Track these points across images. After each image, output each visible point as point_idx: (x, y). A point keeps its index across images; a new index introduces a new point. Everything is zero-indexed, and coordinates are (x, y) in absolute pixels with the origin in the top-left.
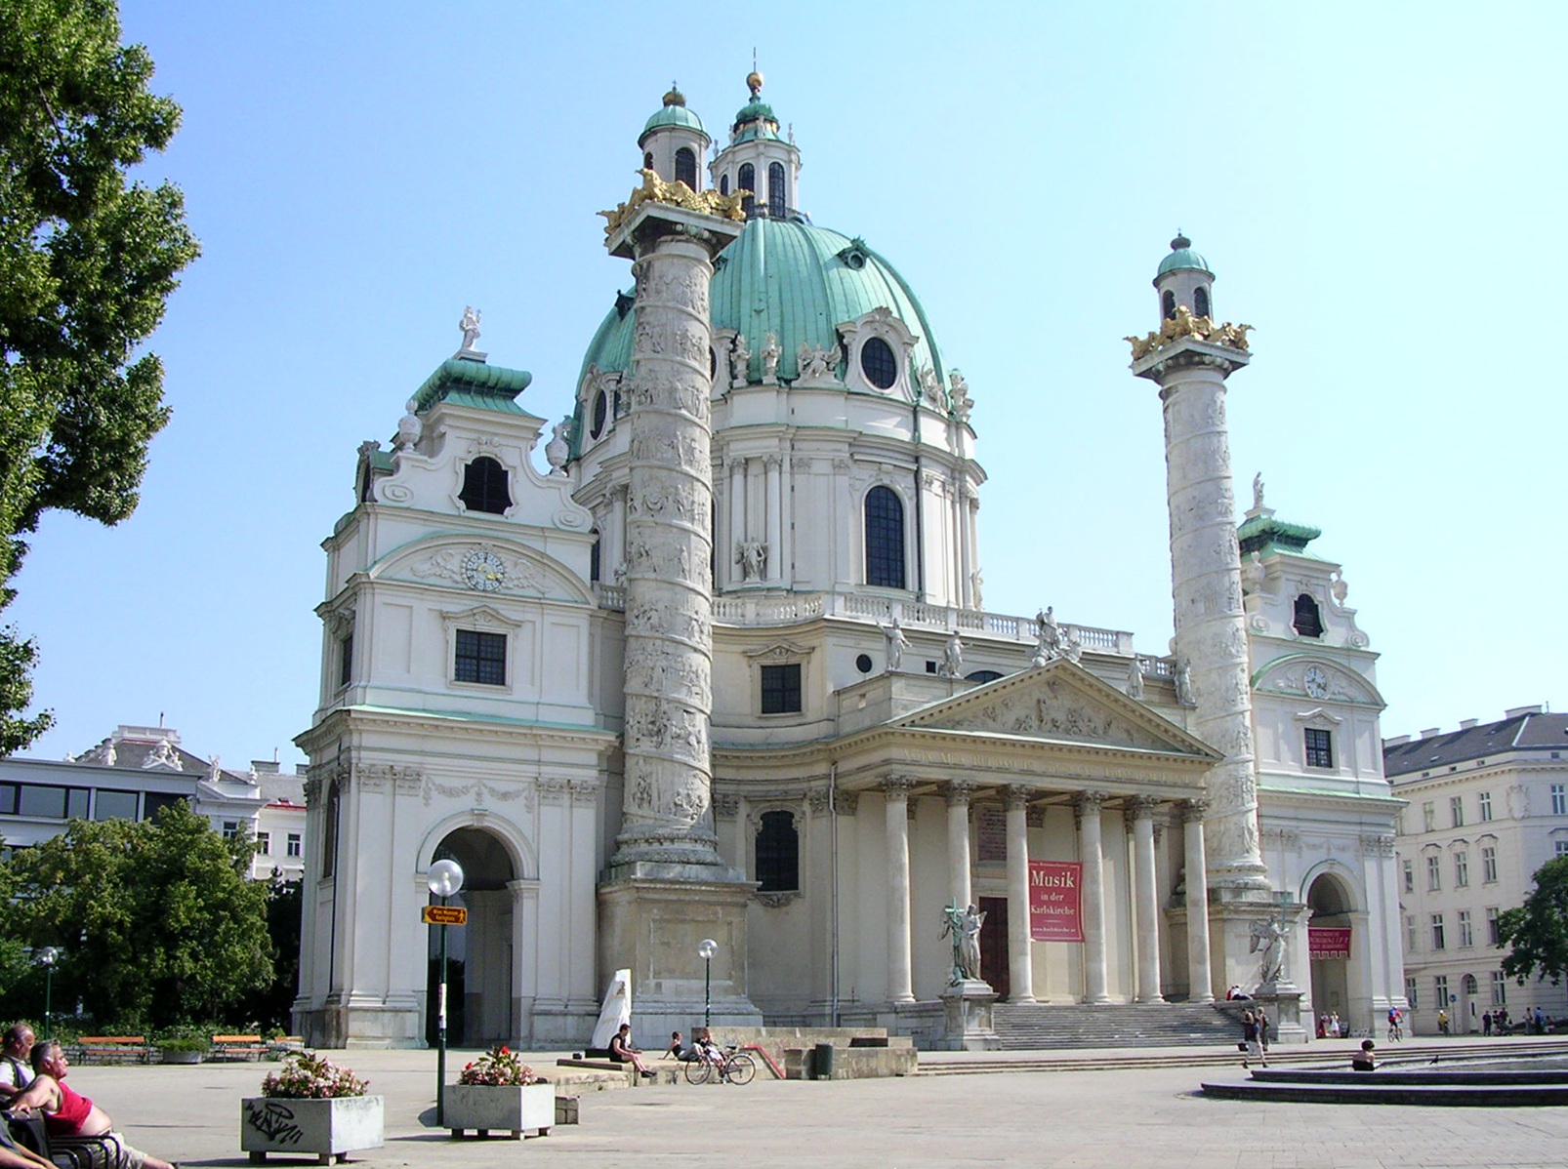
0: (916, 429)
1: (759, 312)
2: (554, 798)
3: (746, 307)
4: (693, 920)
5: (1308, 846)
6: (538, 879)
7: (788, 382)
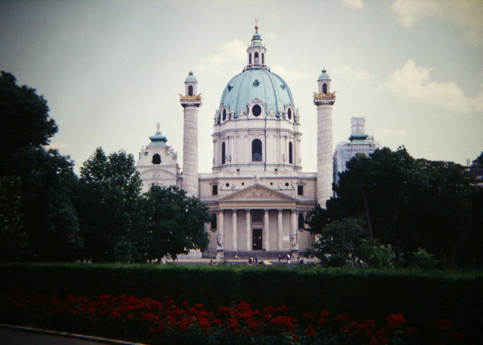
0: (266, 124)
1: (233, 101)
3: (231, 101)
7: (236, 118)
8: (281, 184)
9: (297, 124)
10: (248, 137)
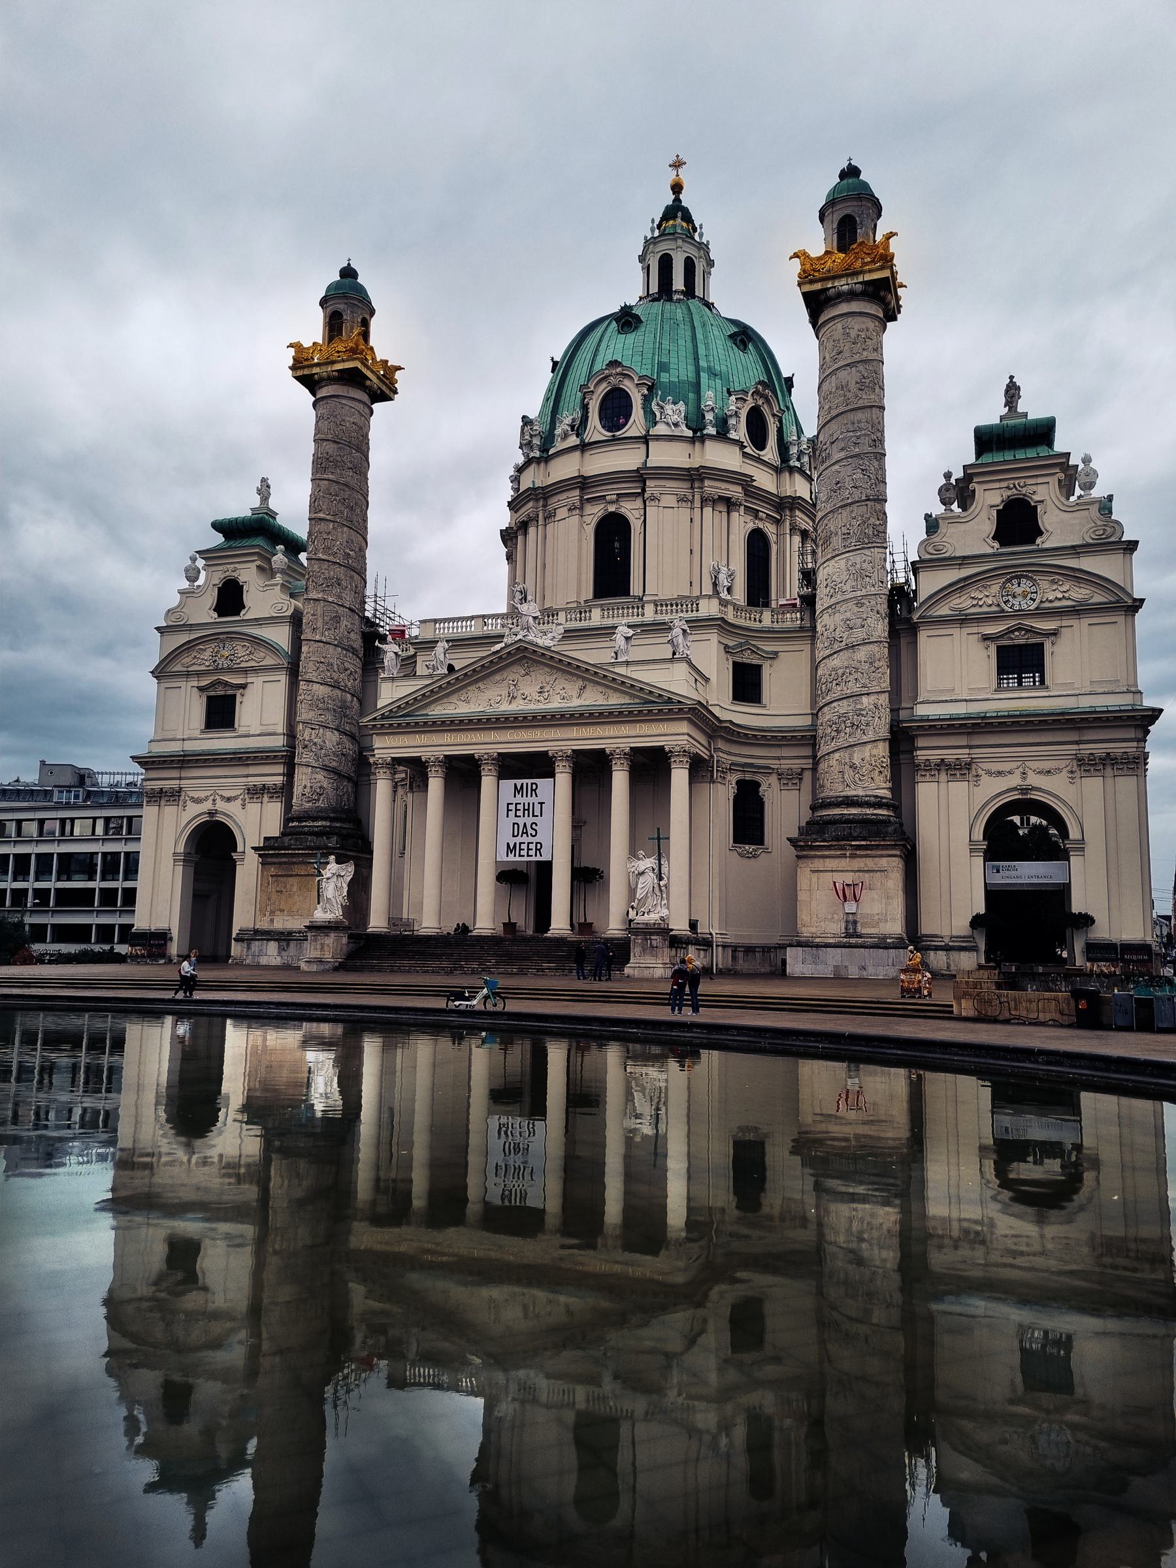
0: (647, 457)
2: (257, 798)
4: (297, 875)
5: (989, 773)
6: (244, 853)
7: (548, 451)
8: (627, 639)
9: (791, 470)
10: (581, 508)
